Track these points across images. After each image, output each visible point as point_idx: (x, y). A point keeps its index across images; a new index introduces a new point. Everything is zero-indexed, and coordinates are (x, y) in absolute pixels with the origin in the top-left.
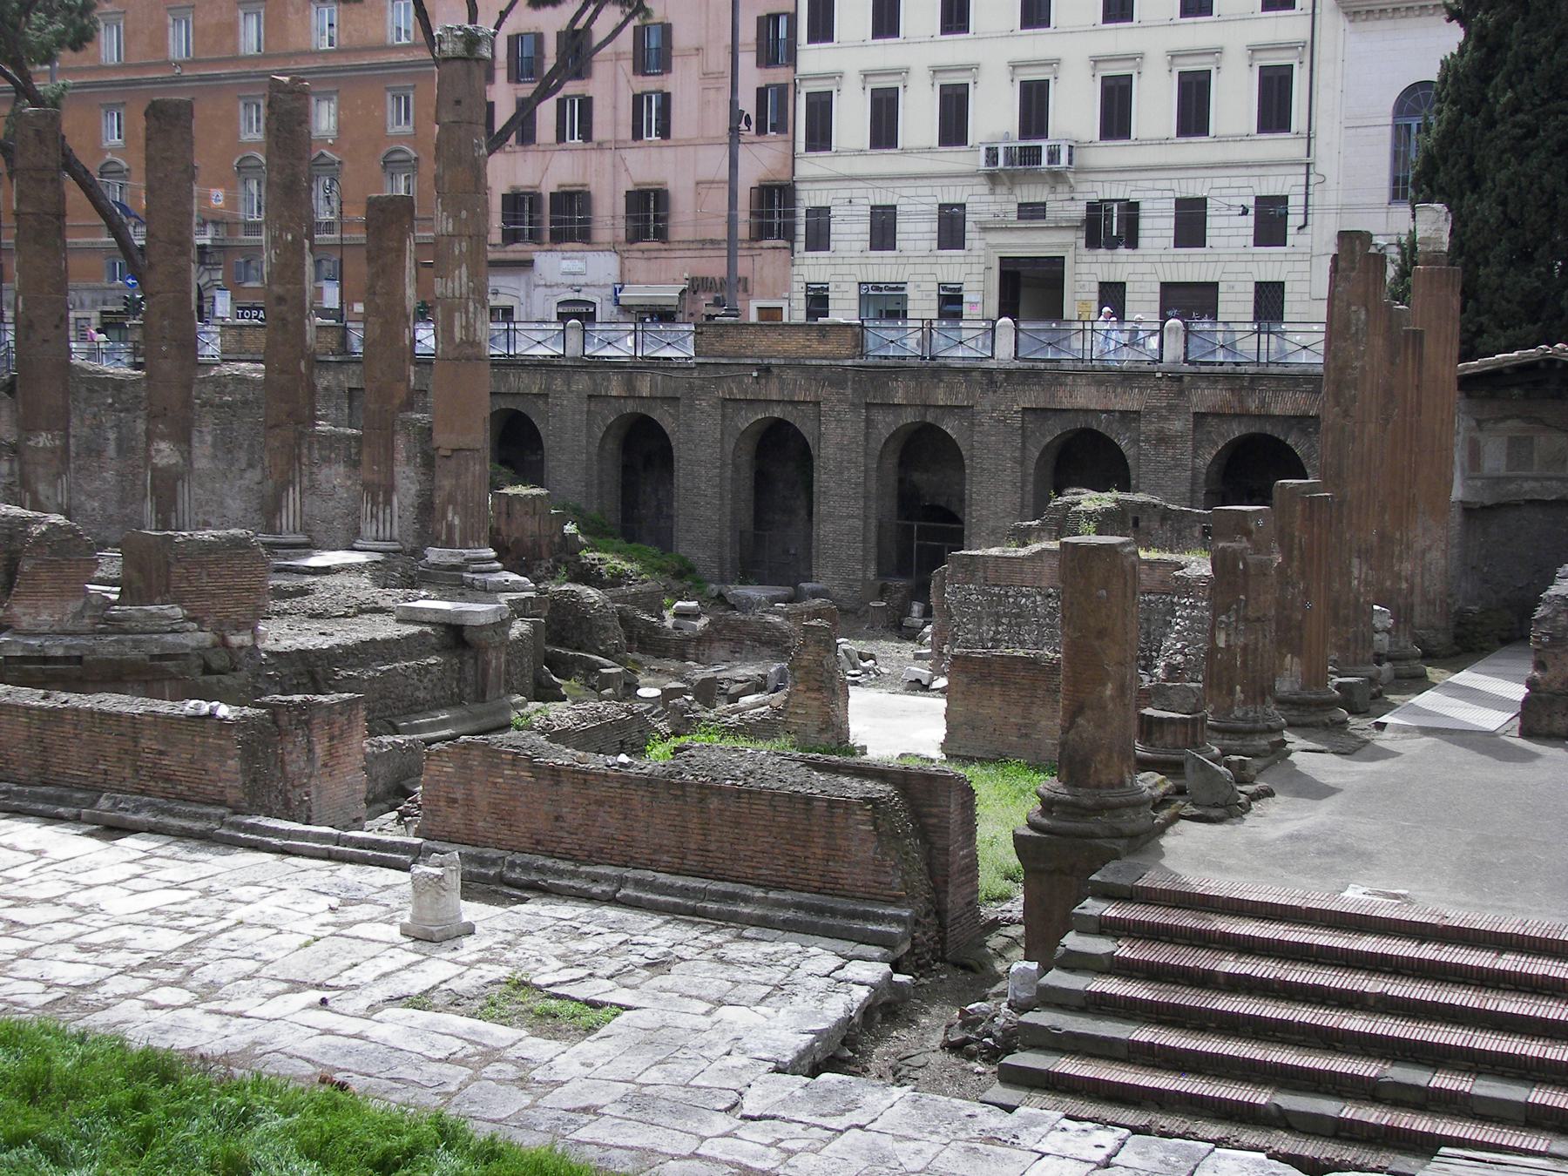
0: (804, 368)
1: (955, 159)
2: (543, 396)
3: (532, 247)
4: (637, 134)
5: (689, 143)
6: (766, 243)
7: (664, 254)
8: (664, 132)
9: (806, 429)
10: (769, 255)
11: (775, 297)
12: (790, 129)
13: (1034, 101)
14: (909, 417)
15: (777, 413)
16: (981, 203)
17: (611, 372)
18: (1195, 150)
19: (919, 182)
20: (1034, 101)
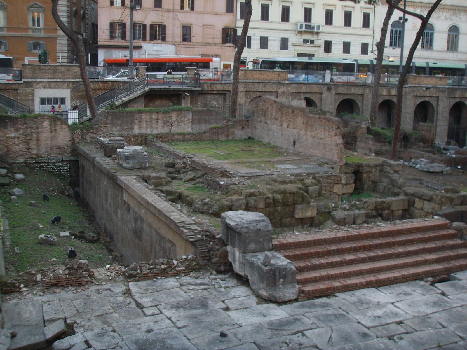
0: (436, 87)
1: (285, 26)
2: (362, 95)
3: (142, 41)
4: (182, 8)
5: (200, 13)
6: (227, 45)
7: (192, 46)
8: (192, 9)
9: (434, 103)
10: (227, 48)
11: (229, 60)
12: (235, 12)
13: (308, 14)
14: (458, 100)
15: (427, 99)
16: (293, 39)
17: (384, 88)
18: (347, 30)
19: (275, 31)
20: (308, 14)
